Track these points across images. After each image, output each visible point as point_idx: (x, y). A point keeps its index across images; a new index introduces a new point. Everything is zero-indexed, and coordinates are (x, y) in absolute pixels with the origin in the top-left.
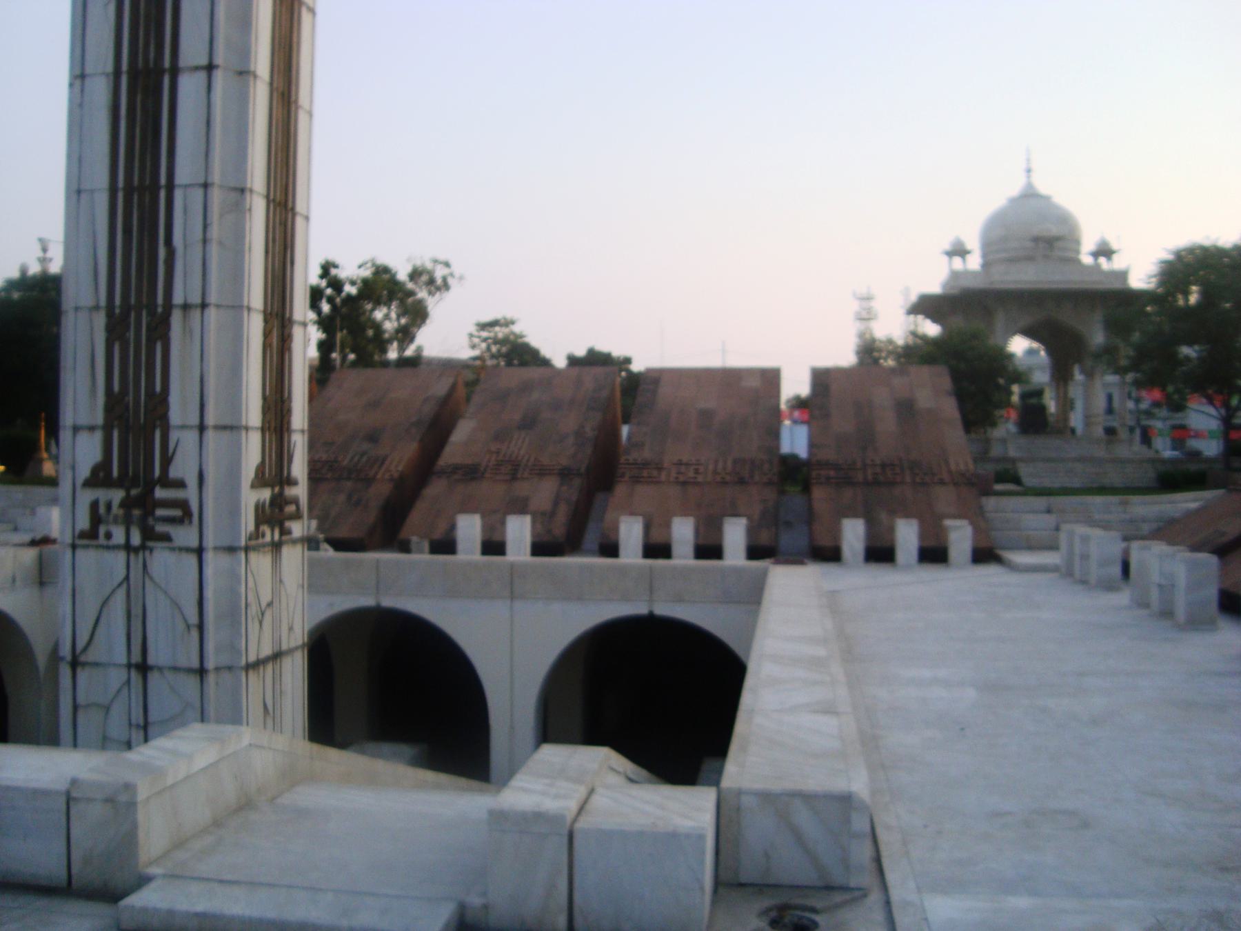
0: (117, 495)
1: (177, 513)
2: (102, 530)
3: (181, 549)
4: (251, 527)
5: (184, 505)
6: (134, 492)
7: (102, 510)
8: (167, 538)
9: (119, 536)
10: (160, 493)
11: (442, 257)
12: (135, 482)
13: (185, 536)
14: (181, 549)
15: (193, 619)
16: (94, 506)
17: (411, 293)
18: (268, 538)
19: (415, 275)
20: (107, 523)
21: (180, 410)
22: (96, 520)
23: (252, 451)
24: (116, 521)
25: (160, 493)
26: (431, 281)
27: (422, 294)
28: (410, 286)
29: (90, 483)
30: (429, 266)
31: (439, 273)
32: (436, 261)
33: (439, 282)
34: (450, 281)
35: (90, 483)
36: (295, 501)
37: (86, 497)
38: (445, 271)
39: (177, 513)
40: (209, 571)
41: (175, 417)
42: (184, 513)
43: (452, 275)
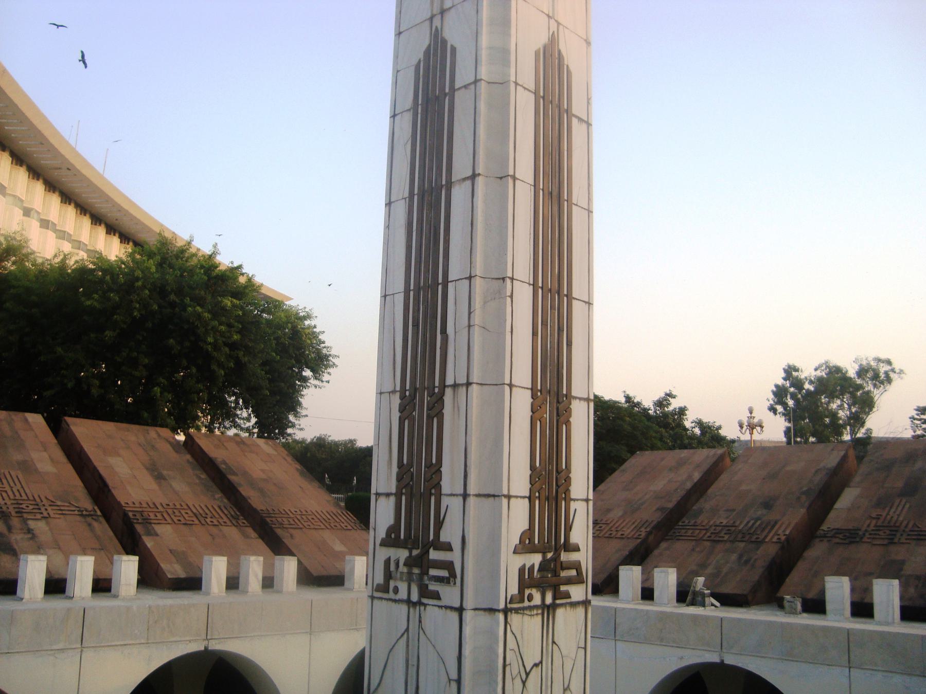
0: (536, 559)
1: (444, 573)
2: (527, 592)
3: (446, 607)
4: (514, 590)
5: (448, 566)
6: (415, 552)
7: (392, 568)
8: (436, 596)
9: (403, 594)
10: (434, 555)
11: (883, 356)
12: (415, 546)
13: (450, 595)
14: (446, 607)
15: (454, 675)
16: (522, 570)
17: (860, 387)
18: (537, 600)
19: (862, 372)
20: (396, 580)
21: (450, 482)
22: (388, 576)
23: (517, 519)
24: (401, 579)
25: (434, 555)
26: (876, 377)
27: (869, 387)
28: (859, 381)
29: (385, 543)
30: (873, 364)
31: (883, 368)
32: (879, 360)
33: (882, 376)
34: (892, 375)
35: (385, 543)
36: (577, 566)
37: (383, 553)
38: (887, 368)
39: (444, 573)
40: (467, 630)
41: (446, 487)
42: (451, 575)
43: (893, 370)
